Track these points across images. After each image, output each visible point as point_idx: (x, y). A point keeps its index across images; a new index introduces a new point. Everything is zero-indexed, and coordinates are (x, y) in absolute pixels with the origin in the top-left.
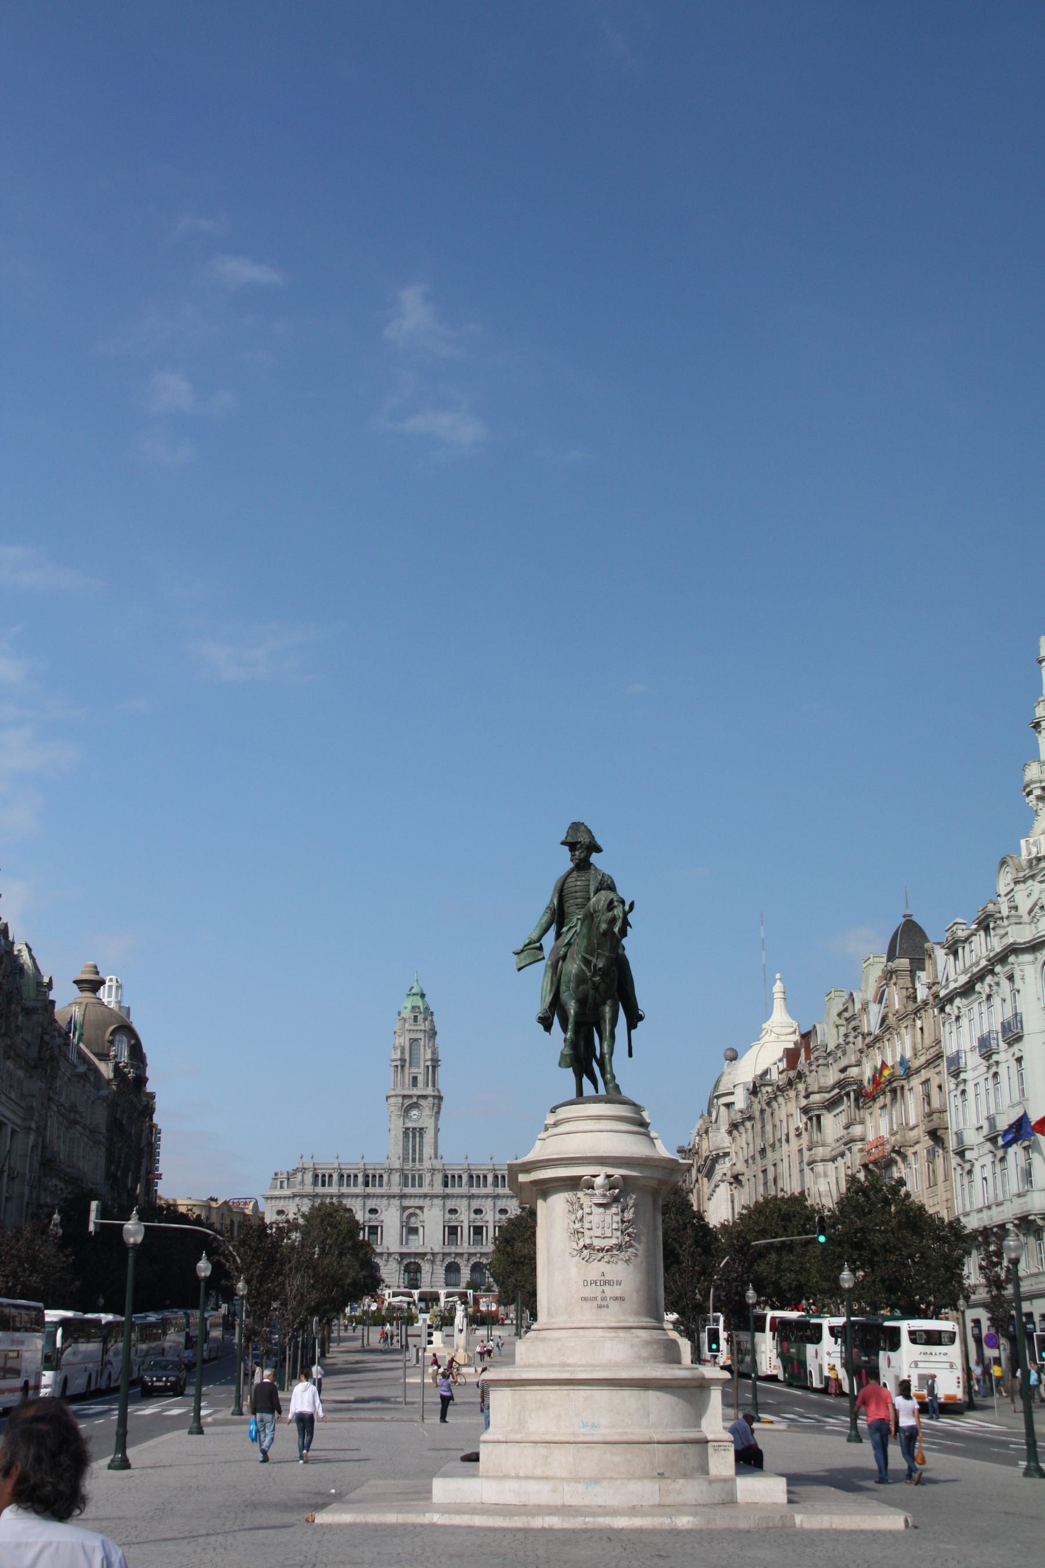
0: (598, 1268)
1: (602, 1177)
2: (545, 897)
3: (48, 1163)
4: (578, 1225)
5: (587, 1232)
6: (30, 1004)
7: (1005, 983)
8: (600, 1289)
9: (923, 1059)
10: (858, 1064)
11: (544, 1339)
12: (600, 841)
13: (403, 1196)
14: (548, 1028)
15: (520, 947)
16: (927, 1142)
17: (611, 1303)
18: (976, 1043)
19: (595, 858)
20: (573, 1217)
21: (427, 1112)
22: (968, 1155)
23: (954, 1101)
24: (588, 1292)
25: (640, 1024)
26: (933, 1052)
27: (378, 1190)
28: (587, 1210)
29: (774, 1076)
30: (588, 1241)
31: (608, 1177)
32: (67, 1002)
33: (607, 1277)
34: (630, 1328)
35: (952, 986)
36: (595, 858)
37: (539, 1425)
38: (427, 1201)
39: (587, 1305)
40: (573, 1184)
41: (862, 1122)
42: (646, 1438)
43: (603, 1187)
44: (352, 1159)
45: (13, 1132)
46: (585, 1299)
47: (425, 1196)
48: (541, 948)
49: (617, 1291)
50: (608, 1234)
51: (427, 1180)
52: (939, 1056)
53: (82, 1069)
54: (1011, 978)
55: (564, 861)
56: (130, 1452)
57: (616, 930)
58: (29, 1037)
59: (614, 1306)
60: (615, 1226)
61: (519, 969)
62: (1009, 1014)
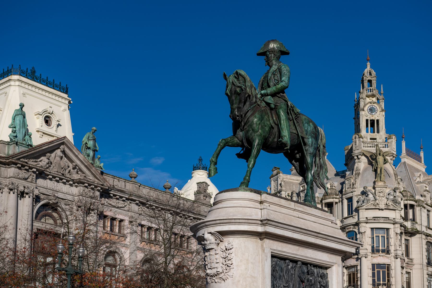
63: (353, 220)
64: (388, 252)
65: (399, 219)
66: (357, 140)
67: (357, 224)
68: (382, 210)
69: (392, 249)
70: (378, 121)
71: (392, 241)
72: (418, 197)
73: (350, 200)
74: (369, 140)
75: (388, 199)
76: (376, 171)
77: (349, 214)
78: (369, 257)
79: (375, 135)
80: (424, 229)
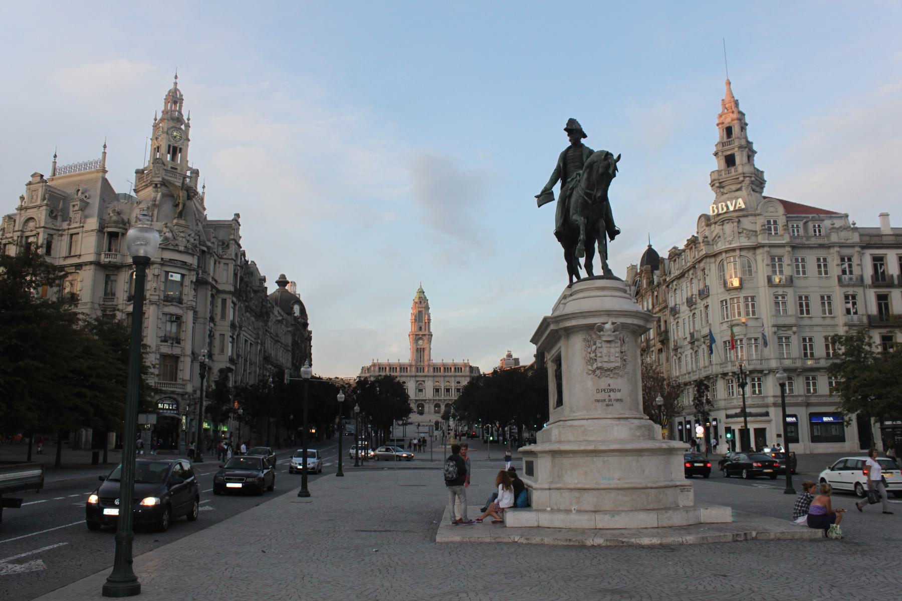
0: (604, 382)
1: (610, 323)
2: (553, 164)
3: (267, 359)
4: (592, 355)
5: (599, 359)
6: (256, 288)
7: (700, 273)
8: (607, 394)
9: (657, 309)
11: (571, 426)
12: (585, 130)
13: (416, 376)
15: (539, 193)
16: (659, 346)
17: (614, 403)
18: (685, 300)
19: (583, 141)
21: (426, 341)
22: (679, 350)
23: (672, 327)
24: (600, 396)
25: (617, 237)
26: (663, 305)
27: (406, 374)
28: (599, 345)
30: (600, 365)
31: (613, 323)
32: (272, 288)
33: (612, 387)
34: (627, 418)
35: (672, 276)
36: (583, 141)
37: (573, 479)
38: (426, 379)
39: (599, 404)
40: (590, 328)
42: (644, 485)
43: (610, 330)
44: (394, 361)
46: (597, 401)
47: (425, 376)
48: (552, 193)
49: (618, 395)
50: (612, 359)
51: (426, 370)
52: (666, 307)
53: (280, 318)
54: (703, 270)
55: (565, 142)
56: (309, 488)
57: (611, 171)
58: (256, 302)
59: (617, 405)
62: (701, 287)
64: (180, 301)
68: (180, 252)
69: (185, 298)
70: (181, 149)
74: (169, 169)
75: (188, 241)
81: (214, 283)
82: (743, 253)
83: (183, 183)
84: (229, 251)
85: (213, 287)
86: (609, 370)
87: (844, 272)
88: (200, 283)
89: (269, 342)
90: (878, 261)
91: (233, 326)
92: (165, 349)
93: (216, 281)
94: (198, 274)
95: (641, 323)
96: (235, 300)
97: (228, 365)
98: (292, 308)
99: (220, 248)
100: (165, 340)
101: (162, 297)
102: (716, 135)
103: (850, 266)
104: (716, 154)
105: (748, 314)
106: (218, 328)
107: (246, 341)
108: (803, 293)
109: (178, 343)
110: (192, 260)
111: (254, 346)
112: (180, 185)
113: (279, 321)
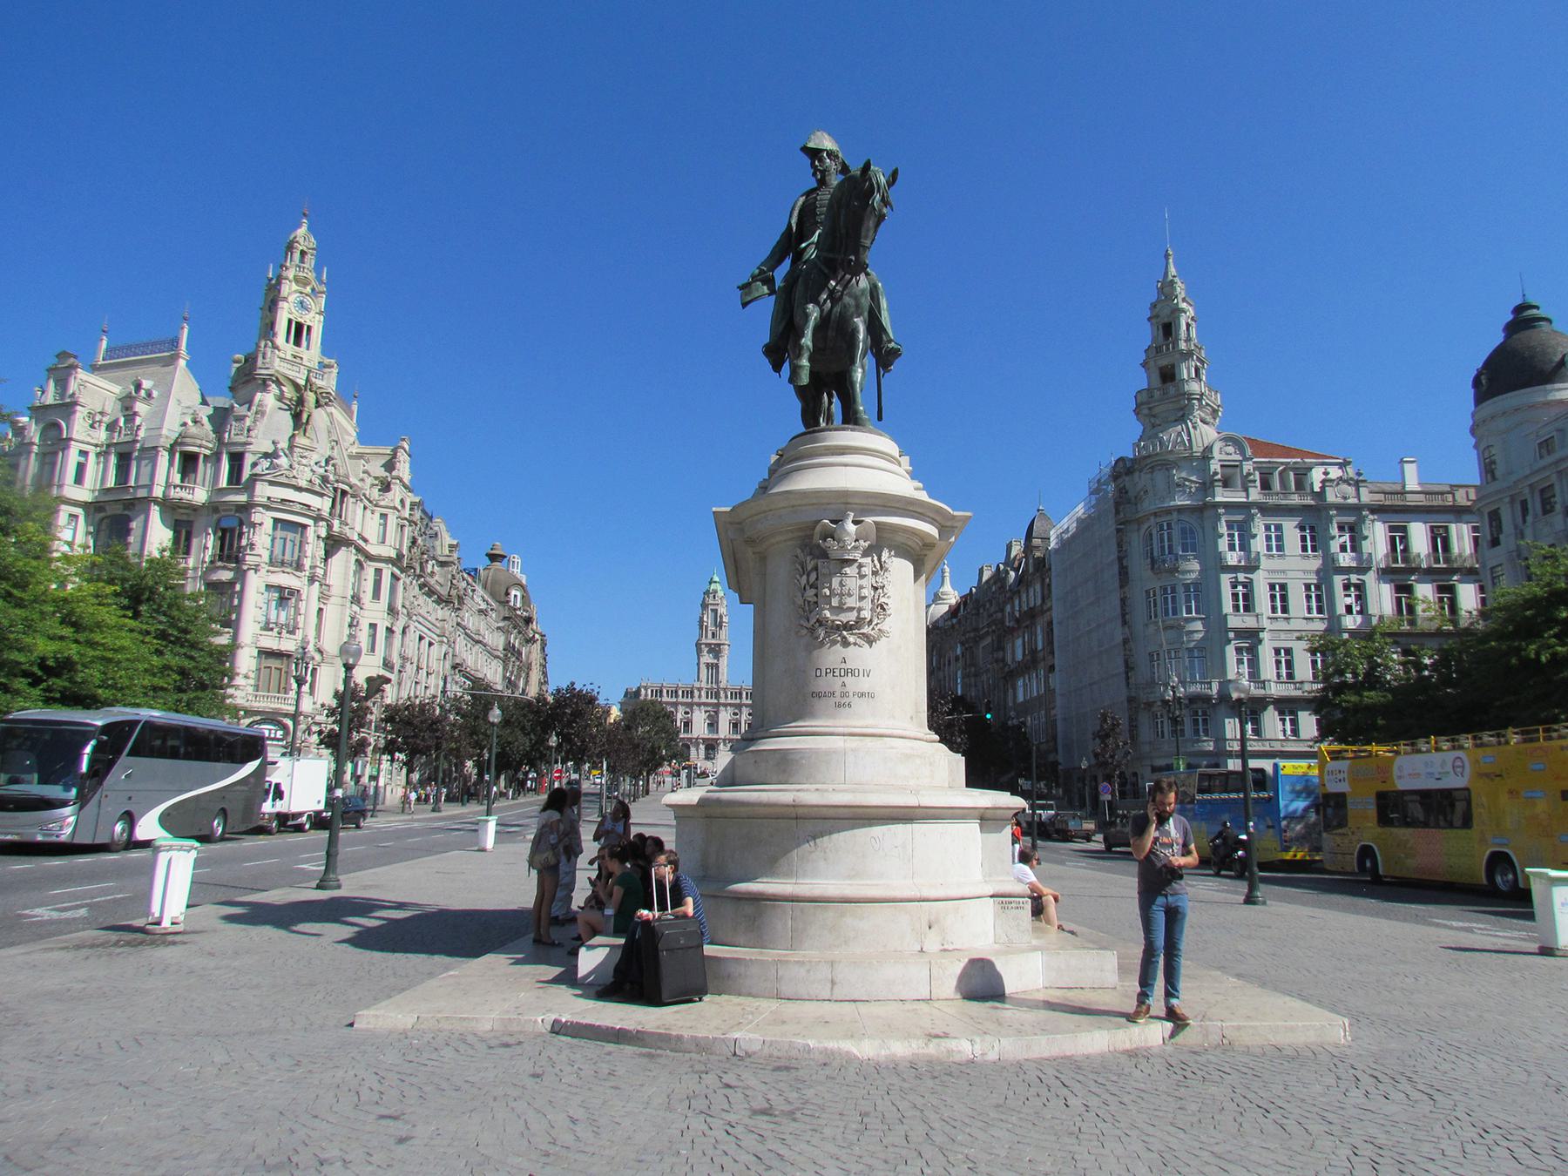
8: (839, 681)
10: (1002, 610)
14: (777, 367)
17: (855, 701)
20: (804, 580)
29: (941, 624)
33: (848, 666)
41: (1003, 649)
45: (431, 644)
49: (863, 684)
50: (851, 602)
53: (483, 606)
58: (441, 581)
60: (865, 592)
61: (745, 305)
63: (243, 498)
64: (299, 567)
65: (326, 513)
66: (269, 351)
67: (247, 508)
68: (299, 489)
69: (307, 563)
71: (309, 549)
72: (353, 480)
73: (237, 459)
76: (297, 417)
77: (230, 482)
78: (263, 572)
79: (302, 351)
80: (356, 537)
81: (361, 542)
82: (1182, 517)
83: (308, 380)
84: (390, 495)
85: (359, 550)
86: (847, 627)
87: (1343, 548)
88: (334, 544)
89: (461, 642)
90: (1399, 536)
91: (392, 610)
92: (270, 642)
93: (366, 541)
94: (330, 527)
95: (931, 530)
96: (397, 572)
97: (382, 672)
98: (507, 594)
99: (376, 490)
100: (267, 627)
101: (266, 558)
102: (1145, 335)
103: (1352, 539)
104: (1144, 365)
105: (1189, 611)
106: (365, 613)
107: (421, 638)
108: (1278, 579)
109: (292, 632)
110: (323, 505)
111: (435, 647)
112: (302, 383)
113: (481, 611)
